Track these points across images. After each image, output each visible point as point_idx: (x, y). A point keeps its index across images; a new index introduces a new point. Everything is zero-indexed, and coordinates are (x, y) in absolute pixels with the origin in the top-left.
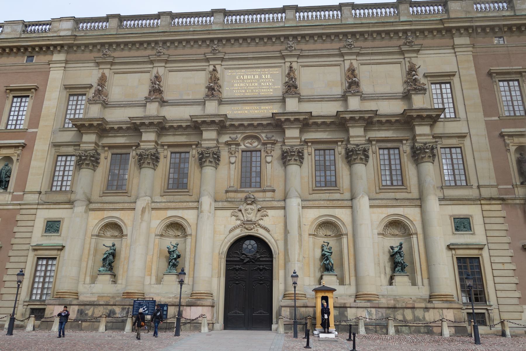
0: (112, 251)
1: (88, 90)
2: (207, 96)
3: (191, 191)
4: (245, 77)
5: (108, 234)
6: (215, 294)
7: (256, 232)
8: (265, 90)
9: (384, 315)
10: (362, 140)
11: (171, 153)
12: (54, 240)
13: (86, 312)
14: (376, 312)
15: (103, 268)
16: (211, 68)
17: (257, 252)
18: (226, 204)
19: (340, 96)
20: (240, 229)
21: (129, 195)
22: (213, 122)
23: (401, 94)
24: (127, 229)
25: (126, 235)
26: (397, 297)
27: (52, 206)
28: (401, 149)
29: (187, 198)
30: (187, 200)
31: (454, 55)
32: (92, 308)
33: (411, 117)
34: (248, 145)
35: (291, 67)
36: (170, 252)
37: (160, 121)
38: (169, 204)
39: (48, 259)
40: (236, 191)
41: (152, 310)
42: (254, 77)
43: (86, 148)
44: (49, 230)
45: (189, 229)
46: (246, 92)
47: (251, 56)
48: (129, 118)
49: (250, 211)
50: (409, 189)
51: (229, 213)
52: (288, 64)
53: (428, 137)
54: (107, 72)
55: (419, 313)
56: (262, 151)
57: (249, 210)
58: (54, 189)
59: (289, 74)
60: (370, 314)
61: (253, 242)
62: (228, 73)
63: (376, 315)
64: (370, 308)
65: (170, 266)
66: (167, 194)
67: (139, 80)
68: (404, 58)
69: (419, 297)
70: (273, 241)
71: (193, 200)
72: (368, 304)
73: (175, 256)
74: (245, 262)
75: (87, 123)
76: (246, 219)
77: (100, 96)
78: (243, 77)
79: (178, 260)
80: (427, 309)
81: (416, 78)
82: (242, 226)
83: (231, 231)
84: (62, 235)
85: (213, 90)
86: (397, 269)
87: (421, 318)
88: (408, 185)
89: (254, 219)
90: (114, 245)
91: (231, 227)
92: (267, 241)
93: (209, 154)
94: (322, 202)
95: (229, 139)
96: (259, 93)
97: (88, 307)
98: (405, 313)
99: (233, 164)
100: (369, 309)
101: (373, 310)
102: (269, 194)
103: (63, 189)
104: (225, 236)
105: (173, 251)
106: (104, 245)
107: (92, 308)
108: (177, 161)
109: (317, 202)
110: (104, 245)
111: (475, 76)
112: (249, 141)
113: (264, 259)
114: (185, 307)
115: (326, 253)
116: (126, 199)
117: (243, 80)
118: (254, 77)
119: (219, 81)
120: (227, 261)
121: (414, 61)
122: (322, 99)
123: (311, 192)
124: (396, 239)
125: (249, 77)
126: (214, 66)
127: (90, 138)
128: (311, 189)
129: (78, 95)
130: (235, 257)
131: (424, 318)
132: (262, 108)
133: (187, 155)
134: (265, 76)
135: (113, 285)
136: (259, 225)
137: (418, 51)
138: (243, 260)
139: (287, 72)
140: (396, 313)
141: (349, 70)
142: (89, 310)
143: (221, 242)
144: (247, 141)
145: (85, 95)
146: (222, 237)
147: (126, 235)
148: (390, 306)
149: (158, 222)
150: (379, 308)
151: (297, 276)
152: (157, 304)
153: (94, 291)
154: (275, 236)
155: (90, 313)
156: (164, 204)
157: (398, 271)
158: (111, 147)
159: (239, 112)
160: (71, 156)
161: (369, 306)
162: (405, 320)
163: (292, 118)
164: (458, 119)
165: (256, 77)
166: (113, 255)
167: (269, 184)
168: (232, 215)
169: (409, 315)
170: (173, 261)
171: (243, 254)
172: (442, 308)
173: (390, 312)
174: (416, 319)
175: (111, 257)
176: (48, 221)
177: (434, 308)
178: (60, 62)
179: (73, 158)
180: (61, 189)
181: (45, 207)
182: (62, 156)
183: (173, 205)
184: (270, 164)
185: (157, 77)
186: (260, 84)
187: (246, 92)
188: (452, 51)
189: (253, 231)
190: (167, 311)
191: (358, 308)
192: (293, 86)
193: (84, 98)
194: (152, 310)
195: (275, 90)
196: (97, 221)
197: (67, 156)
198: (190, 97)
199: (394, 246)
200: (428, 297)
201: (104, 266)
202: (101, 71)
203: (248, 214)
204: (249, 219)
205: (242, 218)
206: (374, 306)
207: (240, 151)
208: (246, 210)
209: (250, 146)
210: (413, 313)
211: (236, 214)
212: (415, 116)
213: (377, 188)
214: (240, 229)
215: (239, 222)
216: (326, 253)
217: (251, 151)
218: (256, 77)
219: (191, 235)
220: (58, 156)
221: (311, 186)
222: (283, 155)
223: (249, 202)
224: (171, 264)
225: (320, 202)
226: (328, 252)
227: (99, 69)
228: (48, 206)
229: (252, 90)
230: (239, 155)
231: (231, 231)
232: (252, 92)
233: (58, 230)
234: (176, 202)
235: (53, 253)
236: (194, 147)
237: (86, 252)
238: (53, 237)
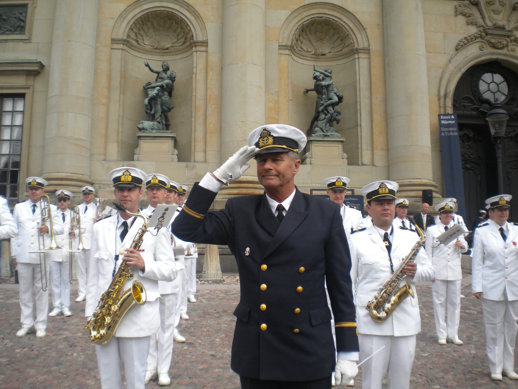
5: (147, 42)
15: (151, 123)
20: (478, 45)
24: (204, 28)
25: (205, 43)
45: (359, 36)
73: (336, 99)
79: (337, 108)
82: (481, 37)
84: (34, 39)
90: (166, 69)
105: (328, 87)
106: (147, 65)
135: (183, 164)
146: (442, 60)
149: (283, 14)
166: (169, 90)
175: (166, 97)
189: (504, 51)
196: (122, 7)
201: (152, 118)
204: (500, 23)
211: (467, 11)
214: (478, 45)
215: (473, 30)
237: (103, 80)
238: (10, 45)
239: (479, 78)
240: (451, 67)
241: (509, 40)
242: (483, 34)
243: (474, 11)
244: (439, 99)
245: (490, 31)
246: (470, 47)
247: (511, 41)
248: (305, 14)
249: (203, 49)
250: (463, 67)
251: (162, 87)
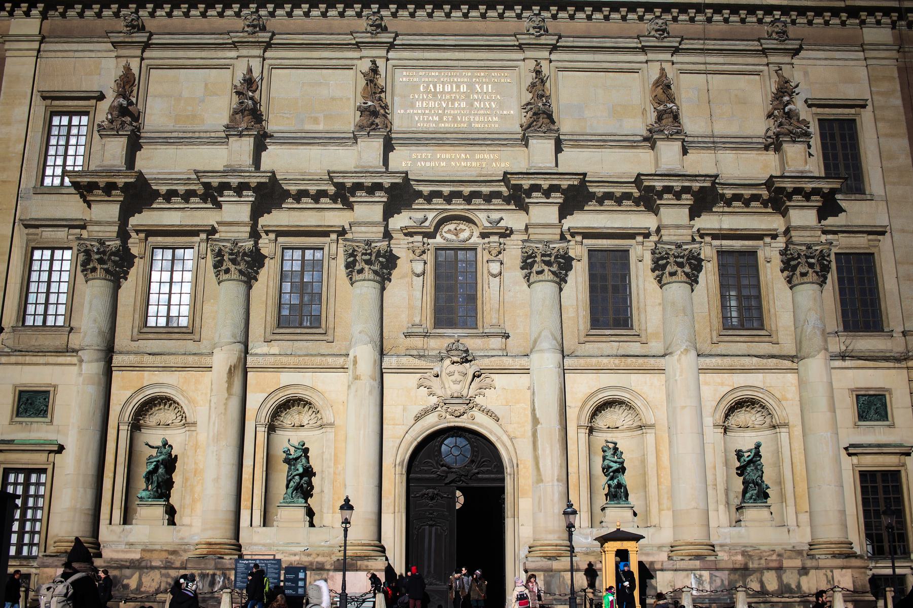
0: (162, 457)
1: (93, 102)
2: (361, 127)
3: (330, 332)
4: (439, 88)
8: (482, 119)
9: (726, 583)
10: (684, 236)
11: (283, 249)
12: (37, 431)
13: (126, 582)
14: (711, 578)
16: (366, 65)
17: (472, 461)
18: (406, 361)
19: (639, 138)
21: (197, 337)
22: (378, 187)
23: (761, 140)
25: (194, 424)
26: (748, 549)
27: (28, 359)
28: (760, 254)
29: (324, 348)
30: (322, 352)
31: (864, 63)
32: (137, 575)
33: (782, 190)
34: (449, 236)
35: (538, 72)
36: (287, 461)
37: (263, 180)
38: (284, 359)
39: (28, 472)
40: (426, 335)
41: (274, 578)
42: (458, 87)
43: (100, 234)
44: (26, 411)
45: (328, 412)
46: (441, 119)
47: (452, 40)
48: (196, 172)
49: (457, 376)
50: (774, 335)
51: (412, 380)
52: (532, 64)
53: (812, 233)
54: (134, 65)
55: (790, 578)
56: (479, 250)
57: (456, 373)
58: (29, 321)
59: (533, 85)
60: (700, 580)
61: (461, 442)
62: (403, 77)
63: (711, 583)
64: (700, 570)
65: (290, 490)
66: (278, 337)
67: (206, 85)
68: (768, 65)
69: (790, 547)
71: (335, 351)
72: (697, 563)
73: (301, 470)
74: (447, 481)
75: (102, 181)
76: (449, 393)
77: (127, 119)
78: (435, 87)
80: (804, 571)
81: (790, 110)
83: (418, 419)
85: (374, 116)
86: (748, 495)
87: (793, 586)
88: (774, 328)
89: (465, 393)
90: (165, 444)
91: (416, 410)
92: (493, 438)
93: (370, 254)
94: (605, 360)
95: (412, 223)
96: (470, 123)
97: (127, 572)
98: (764, 579)
99: (418, 276)
100: (698, 572)
101: (706, 574)
102: (496, 342)
103: (50, 321)
107: (137, 575)
108: (297, 267)
109: (594, 360)
110: (147, 444)
111: (902, 110)
112: (451, 226)
113: (487, 476)
114: (331, 573)
115: (612, 464)
116: (190, 346)
117: (435, 94)
118: (458, 87)
119: (383, 95)
121: (786, 71)
122: (603, 142)
123: (582, 339)
124: (745, 434)
125: (448, 88)
126: (374, 62)
127: (107, 212)
128: (583, 333)
129: (71, 114)
130: (426, 472)
131: (799, 586)
132: (477, 156)
133: (318, 255)
134: (481, 88)
137: (796, 52)
138: (441, 478)
139: (529, 81)
140: (748, 579)
141: (657, 84)
142: (129, 578)
143: (398, 441)
144: (446, 228)
145: (86, 113)
147: (194, 424)
148: (737, 566)
150: (717, 570)
151: (574, 512)
152: (284, 566)
153: (132, 539)
154: (510, 428)
155: (133, 583)
156: (272, 359)
157: (751, 498)
158: (151, 233)
159: (428, 164)
160: (63, 249)
161: (698, 567)
162: (763, 592)
163: (545, 184)
164: (869, 197)
165: (463, 88)
167: (494, 321)
168: (420, 386)
169: (771, 583)
170: (297, 477)
172: (832, 569)
173: (737, 576)
174: (784, 589)
176: (21, 392)
177: (817, 568)
178: (28, 38)
179: (68, 254)
180: (45, 321)
181: (13, 359)
182: (43, 249)
183: (291, 361)
184: (497, 279)
185: (249, 82)
186: (472, 105)
187: (441, 119)
188: (861, 55)
190: (304, 580)
191: (676, 570)
192: (544, 113)
193: (85, 120)
194: (274, 578)
195: (503, 117)
197: (53, 249)
198: (321, 127)
199: (744, 450)
200: (807, 547)
202: (123, 62)
203: (455, 382)
205: (439, 392)
206: (706, 566)
207: (432, 250)
208: (451, 374)
209: (454, 237)
210: (780, 578)
211: (427, 383)
212: (789, 190)
213: (715, 334)
214: (436, 414)
215: (433, 400)
216: (612, 464)
217: (456, 250)
218: (463, 88)
219: (331, 425)
220: (34, 249)
221: (582, 327)
222: (524, 261)
223: (455, 359)
224: (292, 484)
225: (600, 359)
226: (616, 462)
227: (117, 57)
228: (20, 359)
229: (454, 117)
230: (429, 257)
231: (418, 419)
232: (455, 120)
233: (46, 411)
234: (299, 356)
235: (38, 460)
236: (334, 236)
239: (442, 443)
242: (442, 404)
243: (435, 383)
245: (447, 401)
248: (281, 395)
249: (193, 428)
251: (158, 461)
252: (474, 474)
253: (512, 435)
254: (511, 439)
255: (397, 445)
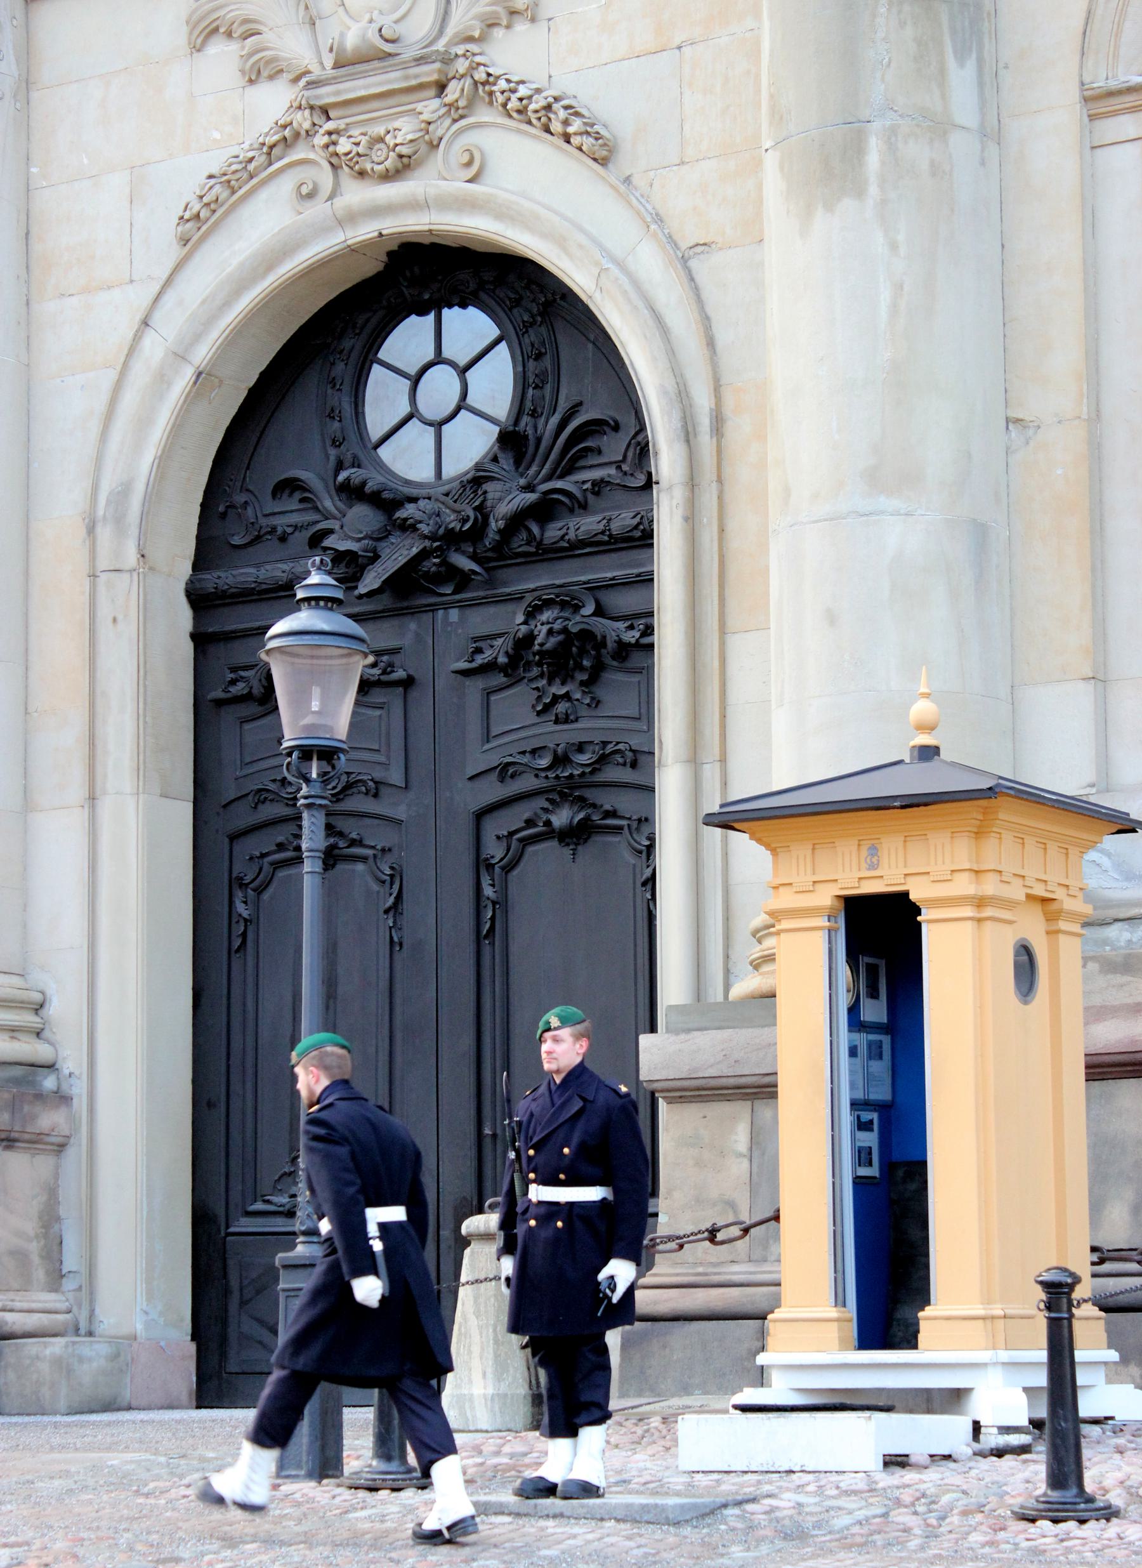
6: (65, 1008)
7: (458, 186)
17: (512, 441)
61: (469, 327)
70: (651, 264)
91: (184, 180)
92: (578, 277)
104: (141, 296)
120: (200, 599)
136: (484, 87)
171: (353, 493)
205: (294, 46)
214: (285, 186)
215: (274, 103)
239: (368, 357)
240: (154, 348)
241: (430, 107)
242: (303, 120)
244: (91, 530)
245: (326, 95)
246: (247, 212)
247: (457, 113)
250: (197, 338)
252: (517, 521)
253: (689, 235)
254: (684, 259)
255: (100, 403)
